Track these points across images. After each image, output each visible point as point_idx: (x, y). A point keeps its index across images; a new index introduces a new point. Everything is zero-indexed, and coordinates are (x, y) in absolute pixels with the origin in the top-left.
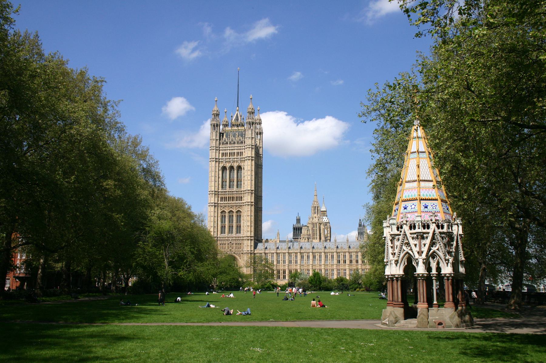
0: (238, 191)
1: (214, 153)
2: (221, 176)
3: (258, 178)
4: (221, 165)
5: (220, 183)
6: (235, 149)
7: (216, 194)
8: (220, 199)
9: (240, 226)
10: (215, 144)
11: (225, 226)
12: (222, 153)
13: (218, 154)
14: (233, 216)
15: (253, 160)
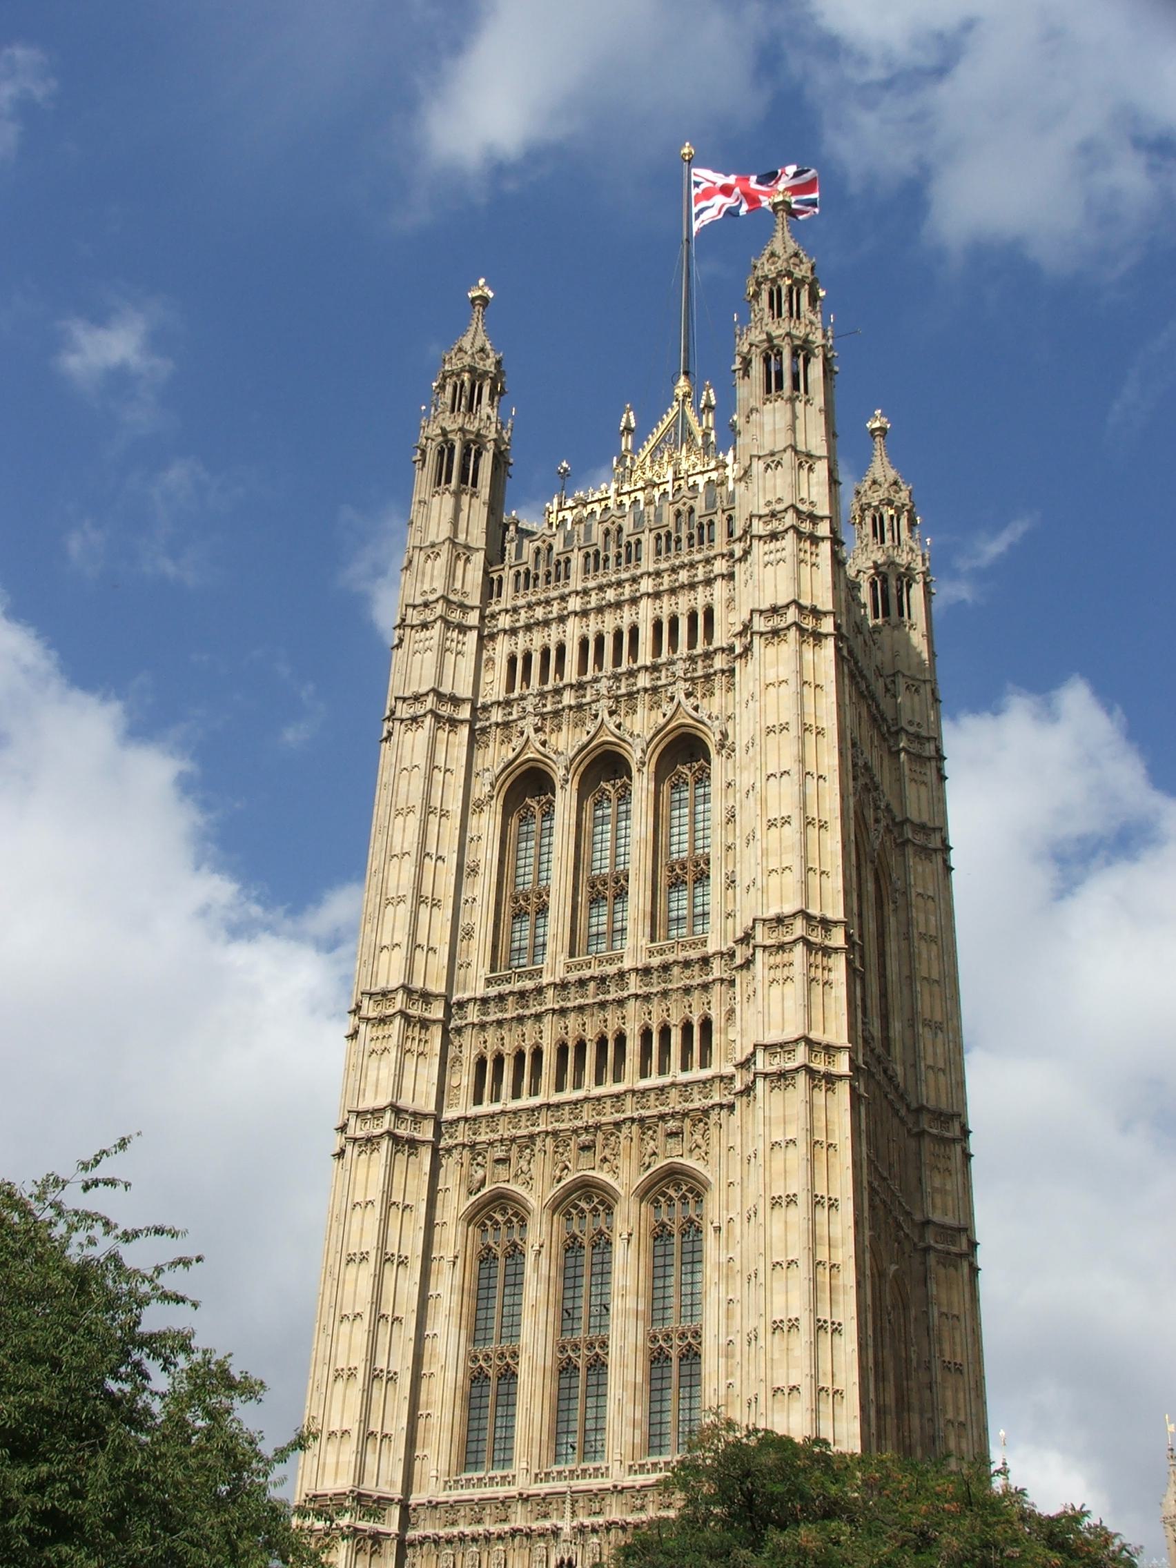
0: (666, 968)
1: (430, 657)
2: (486, 853)
3: (908, 937)
4: (495, 756)
5: (480, 918)
6: (634, 601)
7: (425, 1024)
8: (463, 1078)
9: (692, 1356)
10: (439, 585)
11: (509, 1376)
12: (512, 661)
13: (467, 665)
14: (603, 1243)
15: (818, 637)
